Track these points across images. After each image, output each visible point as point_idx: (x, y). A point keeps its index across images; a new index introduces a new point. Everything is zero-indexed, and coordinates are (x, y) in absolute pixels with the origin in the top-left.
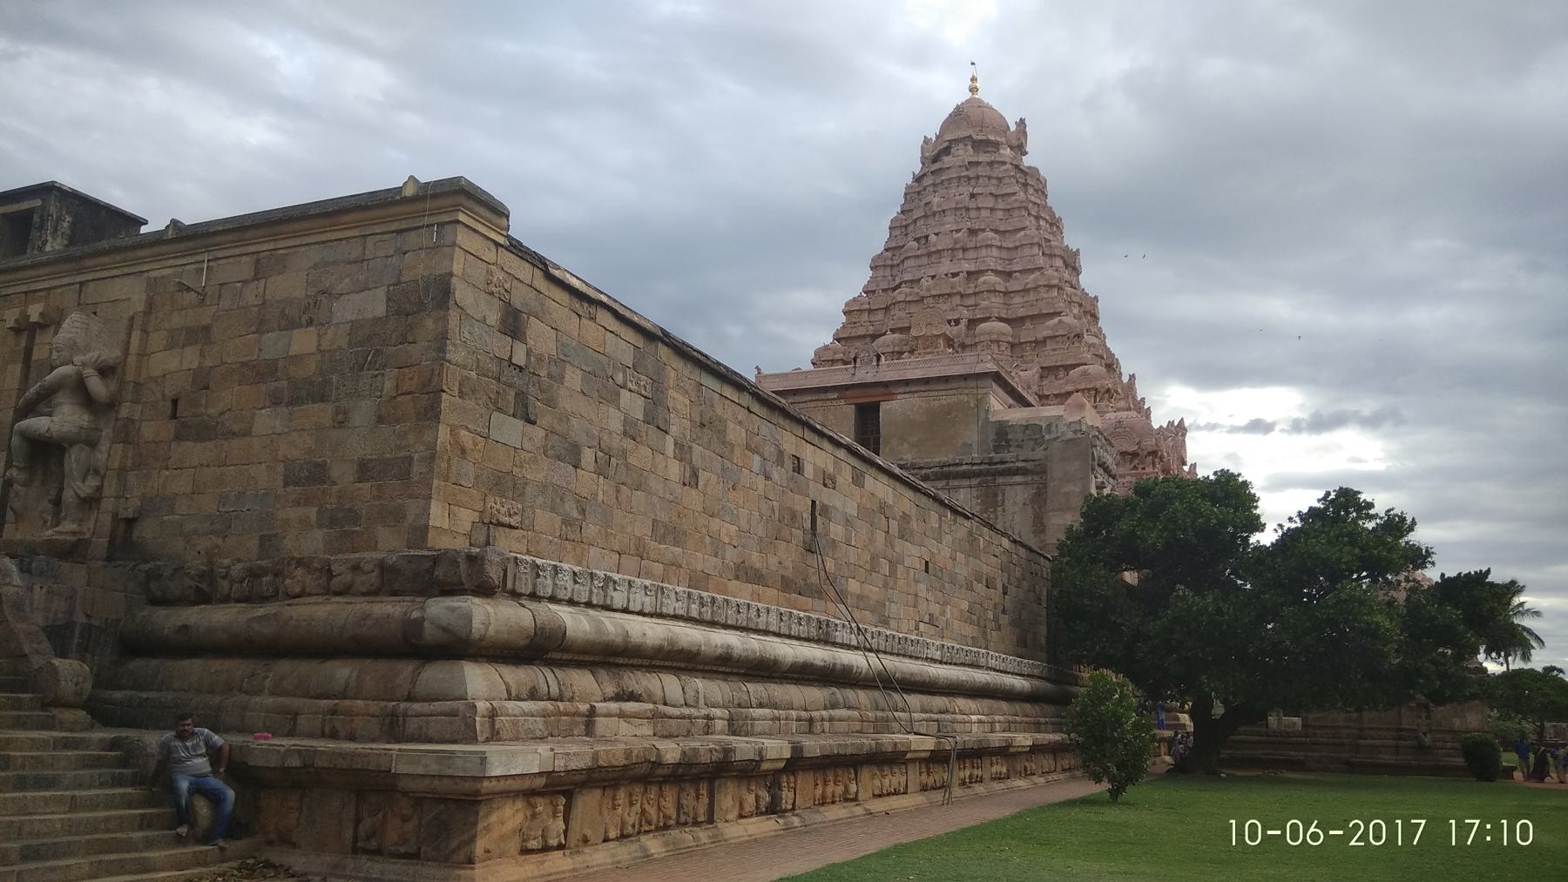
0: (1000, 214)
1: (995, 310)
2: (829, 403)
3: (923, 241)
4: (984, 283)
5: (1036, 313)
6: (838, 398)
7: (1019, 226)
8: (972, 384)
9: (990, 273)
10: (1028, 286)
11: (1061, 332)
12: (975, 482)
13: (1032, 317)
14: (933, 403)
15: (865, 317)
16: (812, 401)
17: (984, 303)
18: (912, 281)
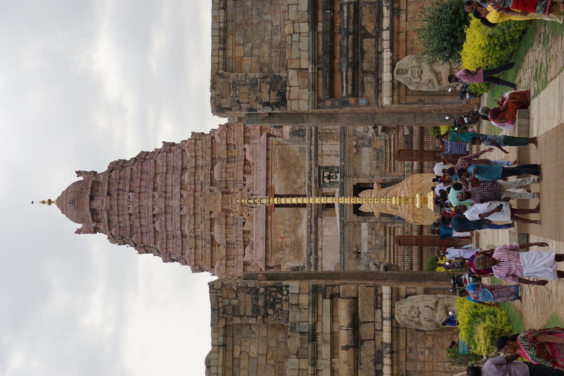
0: (144, 176)
1: (206, 172)
2: (273, 221)
3: (155, 219)
4: (190, 178)
5: (210, 150)
6: (271, 216)
7: (153, 165)
9: (183, 177)
10: (193, 155)
11: (225, 135)
12: (320, 142)
13: (212, 153)
14: (278, 167)
15: (199, 251)
16: (271, 230)
17: (202, 178)
18: (181, 224)
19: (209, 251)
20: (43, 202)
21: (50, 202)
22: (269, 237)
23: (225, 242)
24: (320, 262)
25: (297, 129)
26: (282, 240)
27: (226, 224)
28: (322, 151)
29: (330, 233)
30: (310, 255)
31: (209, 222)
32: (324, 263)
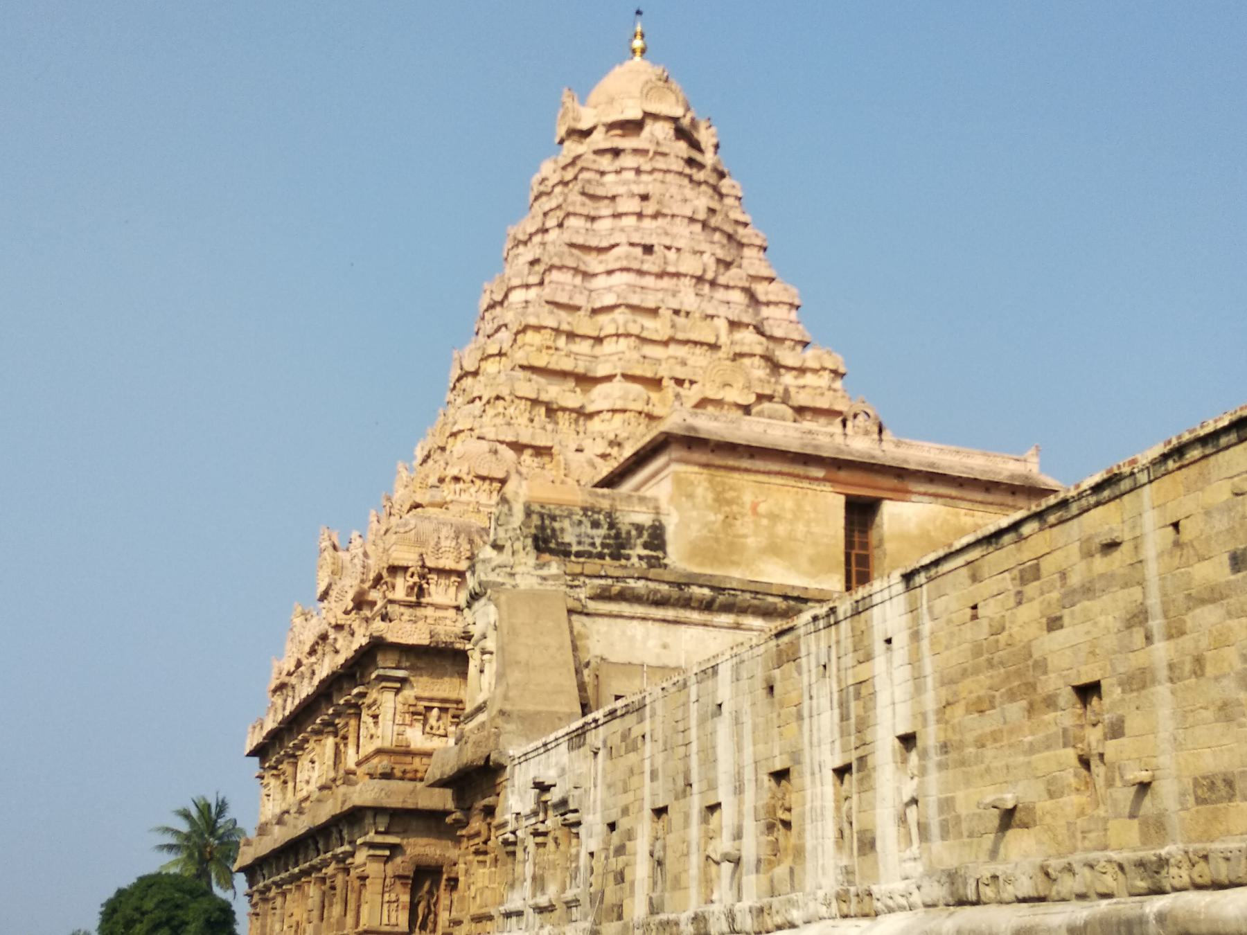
6: (824, 480)
24: (695, 616)
26: (748, 506)
30: (712, 588)
31: (649, 374)
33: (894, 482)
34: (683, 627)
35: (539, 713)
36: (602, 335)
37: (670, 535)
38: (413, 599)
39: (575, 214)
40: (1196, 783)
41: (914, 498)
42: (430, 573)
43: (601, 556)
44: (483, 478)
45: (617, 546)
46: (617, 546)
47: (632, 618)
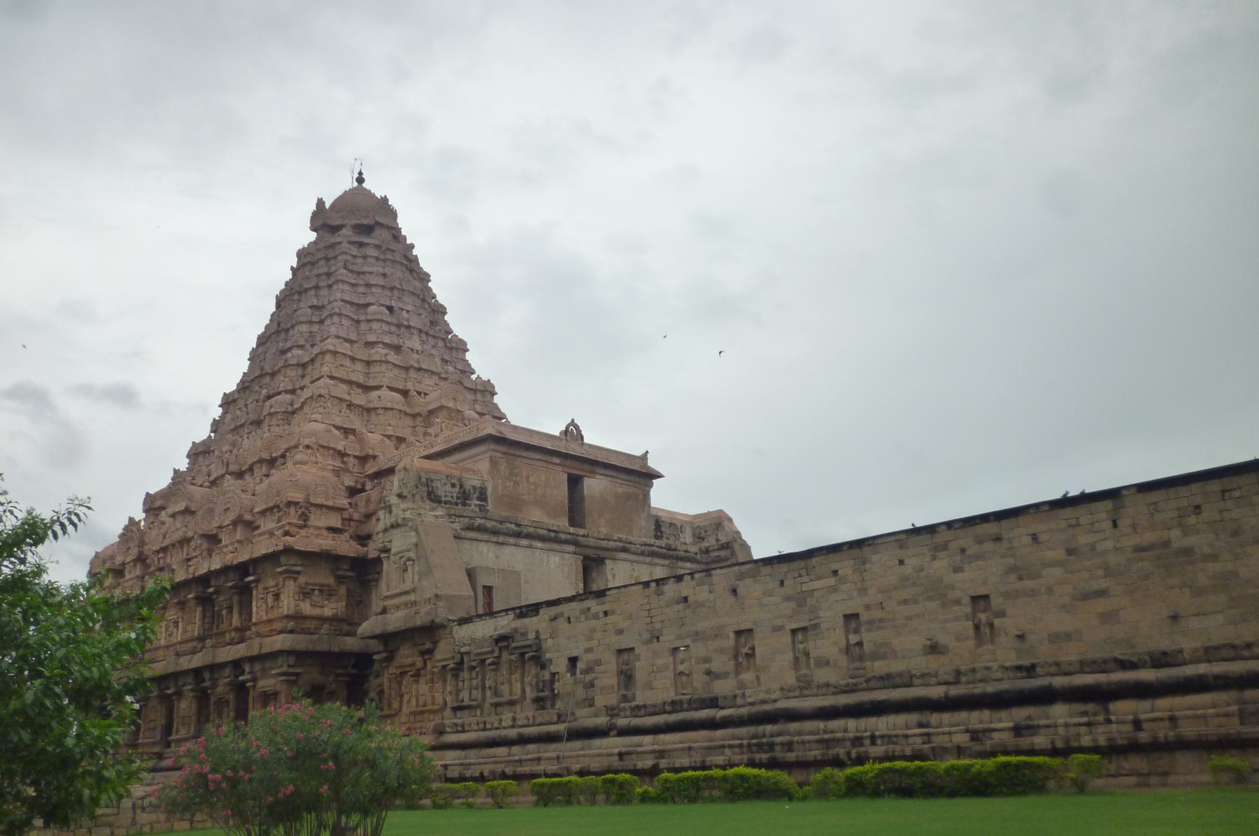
2: (551, 466)
6: (559, 465)
8: (643, 481)
15: (348, 362)
16: (540, 460)
18: (386, 345)
19: (353, 377)
20: (360, 173)
21: (360, 180)
22: (530, 454)
23: (371, 405)
24: (512, 540)
25: (663, 529)
27: (406, 414)
28: (656, 565)
29: (552, 567)
31: (401, 387)
32: (508, 550)
33: (587, 467)
34: (505, 546)
35: (455, 596)
36: (370, 359)
37: (489, 493)
38: (302, 522)
39: (343, 281)
40: (1049, 635)
41: (598, 476)
42: (310, 507)
43: (457, 504)
44: (323, 447)
45: (464, 497)
46: (464, 497)
47: (481, 541)
